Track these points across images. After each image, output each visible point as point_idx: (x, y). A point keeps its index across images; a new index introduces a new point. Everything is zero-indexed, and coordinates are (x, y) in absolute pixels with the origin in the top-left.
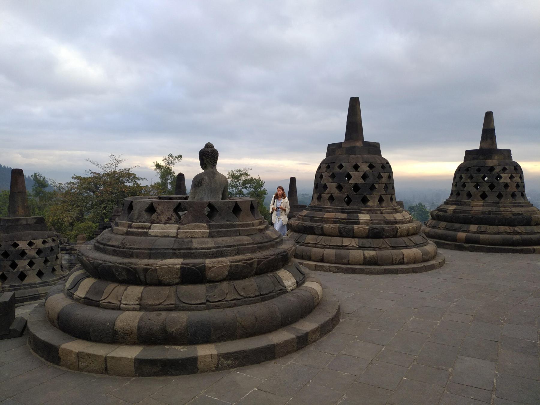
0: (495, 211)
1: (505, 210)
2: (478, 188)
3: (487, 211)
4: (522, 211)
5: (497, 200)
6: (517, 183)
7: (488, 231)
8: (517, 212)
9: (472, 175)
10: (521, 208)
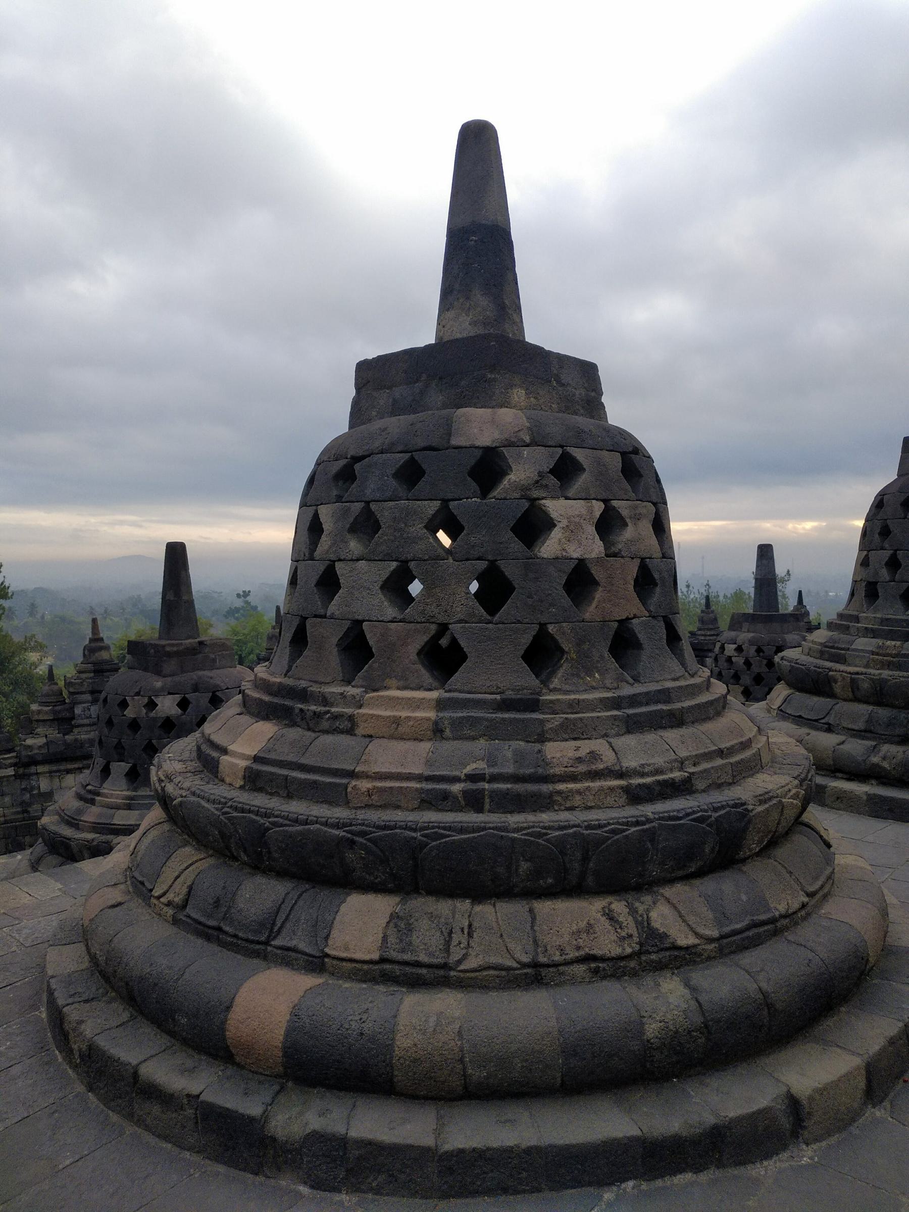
0: (516, 778)
1: (579, 760)
2: (409, 599)
3: (455, 780)
4: (681, 764)
5: (529, 680)
6: (643, 559)
7: (460, 962)
8: (658, 771)
9: (373, 506)
10: (671, 735)
